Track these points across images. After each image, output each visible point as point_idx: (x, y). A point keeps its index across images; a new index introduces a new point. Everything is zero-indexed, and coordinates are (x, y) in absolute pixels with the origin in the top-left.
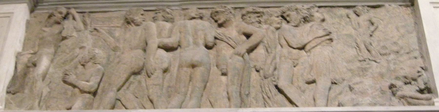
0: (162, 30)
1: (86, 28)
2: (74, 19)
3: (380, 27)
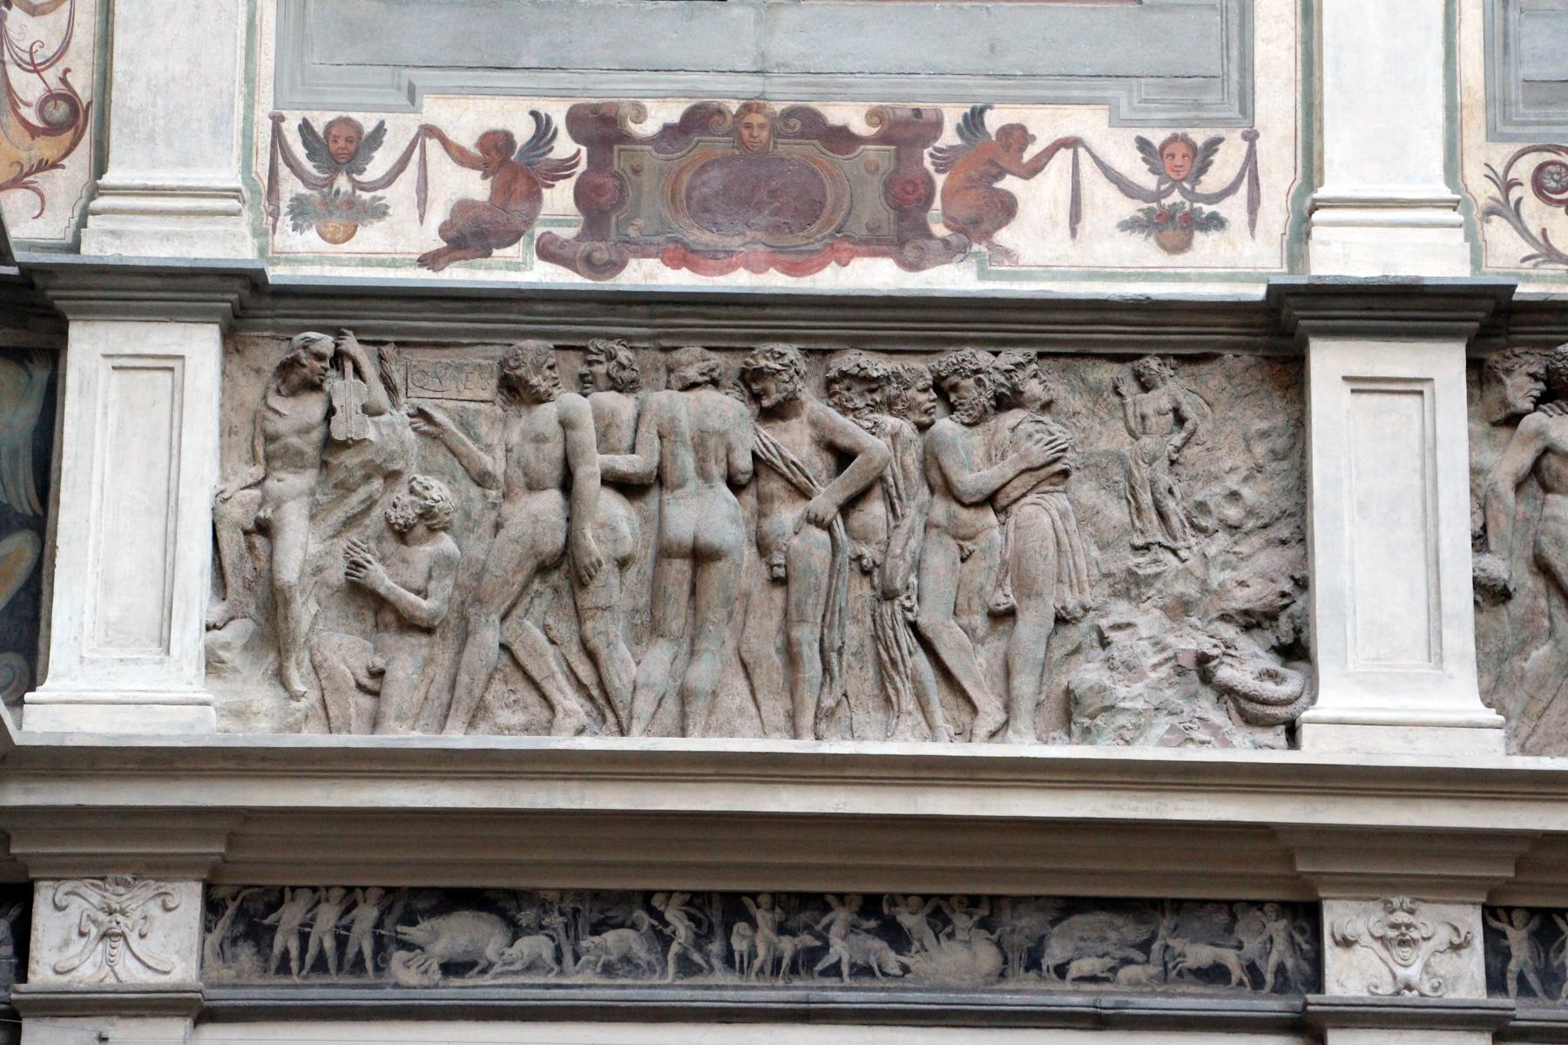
0: (609, 426)
1: (395, 404)
2: (358, 372)
3: (1202, 430)
